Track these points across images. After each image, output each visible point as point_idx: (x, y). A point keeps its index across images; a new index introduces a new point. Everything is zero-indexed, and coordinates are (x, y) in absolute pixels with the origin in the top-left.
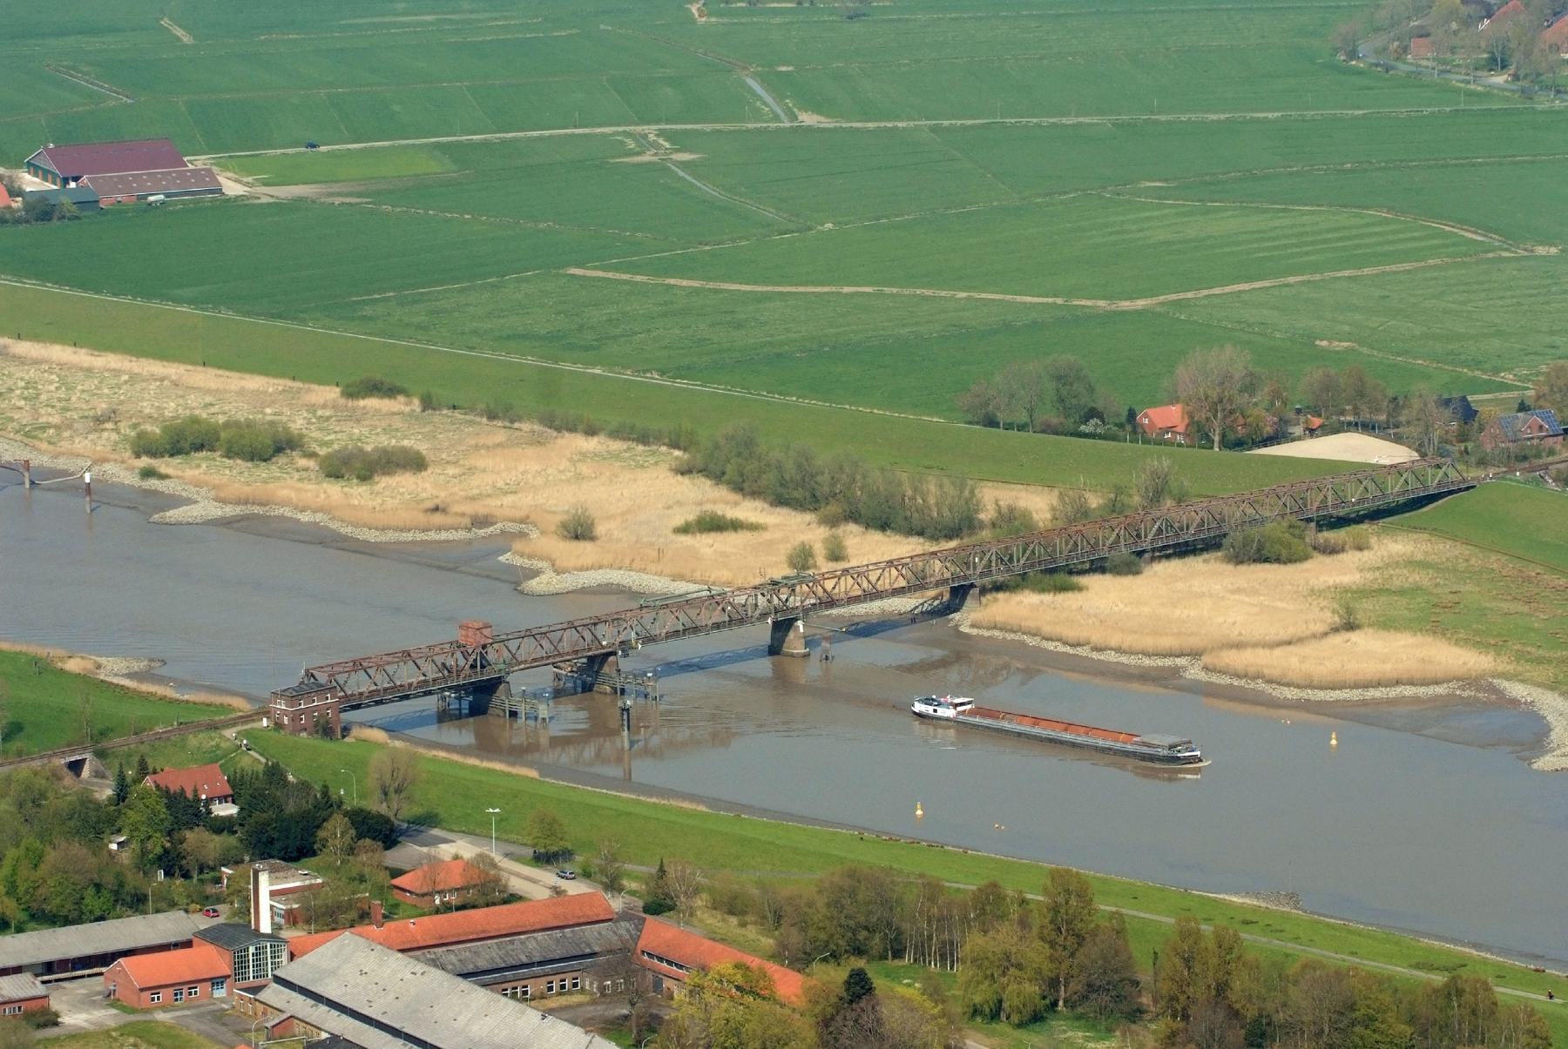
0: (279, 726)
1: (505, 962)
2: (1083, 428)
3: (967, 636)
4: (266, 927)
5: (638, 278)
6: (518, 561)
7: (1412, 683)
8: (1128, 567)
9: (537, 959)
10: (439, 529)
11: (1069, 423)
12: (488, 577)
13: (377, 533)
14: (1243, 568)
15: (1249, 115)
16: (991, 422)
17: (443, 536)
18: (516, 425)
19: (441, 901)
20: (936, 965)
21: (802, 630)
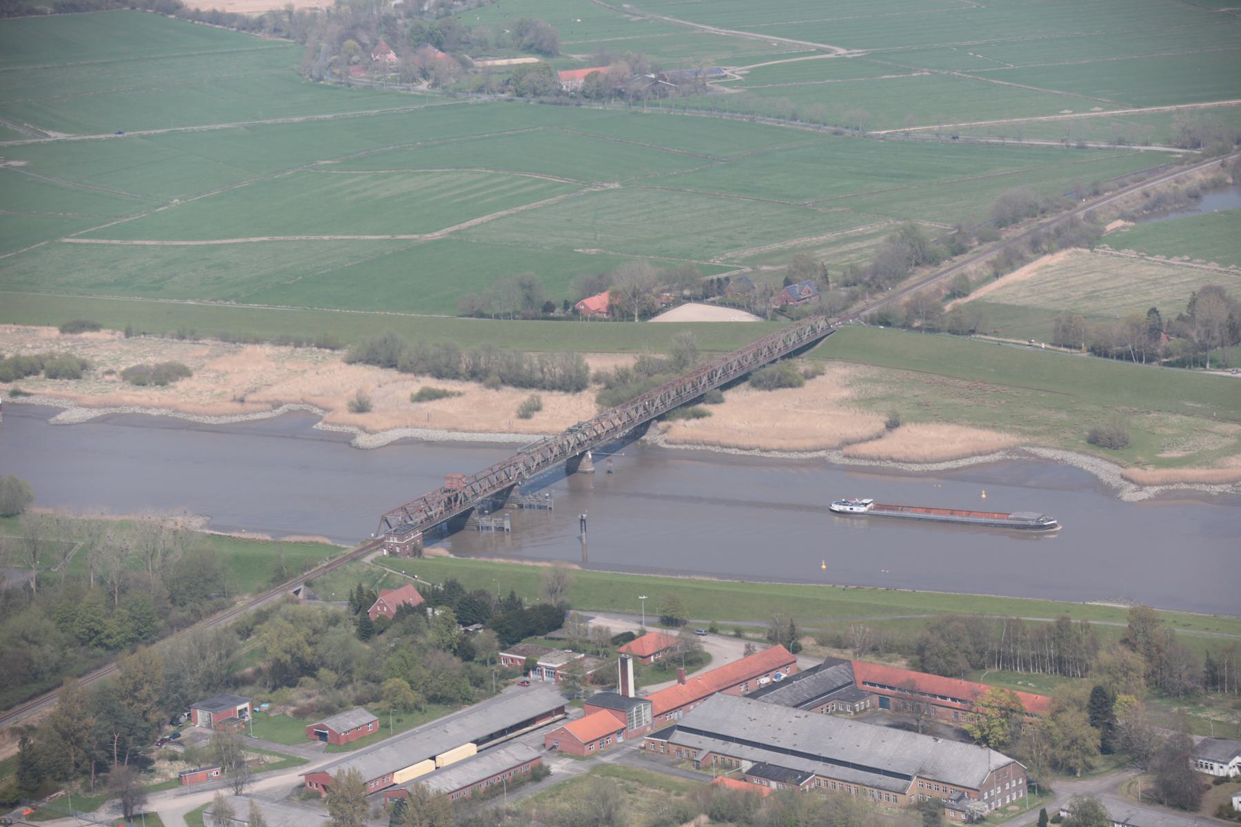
0: (392, 553)
1: (799, 699)
2: (552, 314)
3: (664, 449)
4: (632, 694)
5: (114, 242)
6: (329, 428)
7: (980, 454)
8: (718, 401)
9: (814, 695)
10: (254, 412)
12: (322, 440)
13: (217, 418)
14: (774, 392)
15: (316, 117)
16: (482, 315)
17: (258, 416)
18: (201, 342)
19: (654, 659)
20: (1021, 669)
21: (590, 456)
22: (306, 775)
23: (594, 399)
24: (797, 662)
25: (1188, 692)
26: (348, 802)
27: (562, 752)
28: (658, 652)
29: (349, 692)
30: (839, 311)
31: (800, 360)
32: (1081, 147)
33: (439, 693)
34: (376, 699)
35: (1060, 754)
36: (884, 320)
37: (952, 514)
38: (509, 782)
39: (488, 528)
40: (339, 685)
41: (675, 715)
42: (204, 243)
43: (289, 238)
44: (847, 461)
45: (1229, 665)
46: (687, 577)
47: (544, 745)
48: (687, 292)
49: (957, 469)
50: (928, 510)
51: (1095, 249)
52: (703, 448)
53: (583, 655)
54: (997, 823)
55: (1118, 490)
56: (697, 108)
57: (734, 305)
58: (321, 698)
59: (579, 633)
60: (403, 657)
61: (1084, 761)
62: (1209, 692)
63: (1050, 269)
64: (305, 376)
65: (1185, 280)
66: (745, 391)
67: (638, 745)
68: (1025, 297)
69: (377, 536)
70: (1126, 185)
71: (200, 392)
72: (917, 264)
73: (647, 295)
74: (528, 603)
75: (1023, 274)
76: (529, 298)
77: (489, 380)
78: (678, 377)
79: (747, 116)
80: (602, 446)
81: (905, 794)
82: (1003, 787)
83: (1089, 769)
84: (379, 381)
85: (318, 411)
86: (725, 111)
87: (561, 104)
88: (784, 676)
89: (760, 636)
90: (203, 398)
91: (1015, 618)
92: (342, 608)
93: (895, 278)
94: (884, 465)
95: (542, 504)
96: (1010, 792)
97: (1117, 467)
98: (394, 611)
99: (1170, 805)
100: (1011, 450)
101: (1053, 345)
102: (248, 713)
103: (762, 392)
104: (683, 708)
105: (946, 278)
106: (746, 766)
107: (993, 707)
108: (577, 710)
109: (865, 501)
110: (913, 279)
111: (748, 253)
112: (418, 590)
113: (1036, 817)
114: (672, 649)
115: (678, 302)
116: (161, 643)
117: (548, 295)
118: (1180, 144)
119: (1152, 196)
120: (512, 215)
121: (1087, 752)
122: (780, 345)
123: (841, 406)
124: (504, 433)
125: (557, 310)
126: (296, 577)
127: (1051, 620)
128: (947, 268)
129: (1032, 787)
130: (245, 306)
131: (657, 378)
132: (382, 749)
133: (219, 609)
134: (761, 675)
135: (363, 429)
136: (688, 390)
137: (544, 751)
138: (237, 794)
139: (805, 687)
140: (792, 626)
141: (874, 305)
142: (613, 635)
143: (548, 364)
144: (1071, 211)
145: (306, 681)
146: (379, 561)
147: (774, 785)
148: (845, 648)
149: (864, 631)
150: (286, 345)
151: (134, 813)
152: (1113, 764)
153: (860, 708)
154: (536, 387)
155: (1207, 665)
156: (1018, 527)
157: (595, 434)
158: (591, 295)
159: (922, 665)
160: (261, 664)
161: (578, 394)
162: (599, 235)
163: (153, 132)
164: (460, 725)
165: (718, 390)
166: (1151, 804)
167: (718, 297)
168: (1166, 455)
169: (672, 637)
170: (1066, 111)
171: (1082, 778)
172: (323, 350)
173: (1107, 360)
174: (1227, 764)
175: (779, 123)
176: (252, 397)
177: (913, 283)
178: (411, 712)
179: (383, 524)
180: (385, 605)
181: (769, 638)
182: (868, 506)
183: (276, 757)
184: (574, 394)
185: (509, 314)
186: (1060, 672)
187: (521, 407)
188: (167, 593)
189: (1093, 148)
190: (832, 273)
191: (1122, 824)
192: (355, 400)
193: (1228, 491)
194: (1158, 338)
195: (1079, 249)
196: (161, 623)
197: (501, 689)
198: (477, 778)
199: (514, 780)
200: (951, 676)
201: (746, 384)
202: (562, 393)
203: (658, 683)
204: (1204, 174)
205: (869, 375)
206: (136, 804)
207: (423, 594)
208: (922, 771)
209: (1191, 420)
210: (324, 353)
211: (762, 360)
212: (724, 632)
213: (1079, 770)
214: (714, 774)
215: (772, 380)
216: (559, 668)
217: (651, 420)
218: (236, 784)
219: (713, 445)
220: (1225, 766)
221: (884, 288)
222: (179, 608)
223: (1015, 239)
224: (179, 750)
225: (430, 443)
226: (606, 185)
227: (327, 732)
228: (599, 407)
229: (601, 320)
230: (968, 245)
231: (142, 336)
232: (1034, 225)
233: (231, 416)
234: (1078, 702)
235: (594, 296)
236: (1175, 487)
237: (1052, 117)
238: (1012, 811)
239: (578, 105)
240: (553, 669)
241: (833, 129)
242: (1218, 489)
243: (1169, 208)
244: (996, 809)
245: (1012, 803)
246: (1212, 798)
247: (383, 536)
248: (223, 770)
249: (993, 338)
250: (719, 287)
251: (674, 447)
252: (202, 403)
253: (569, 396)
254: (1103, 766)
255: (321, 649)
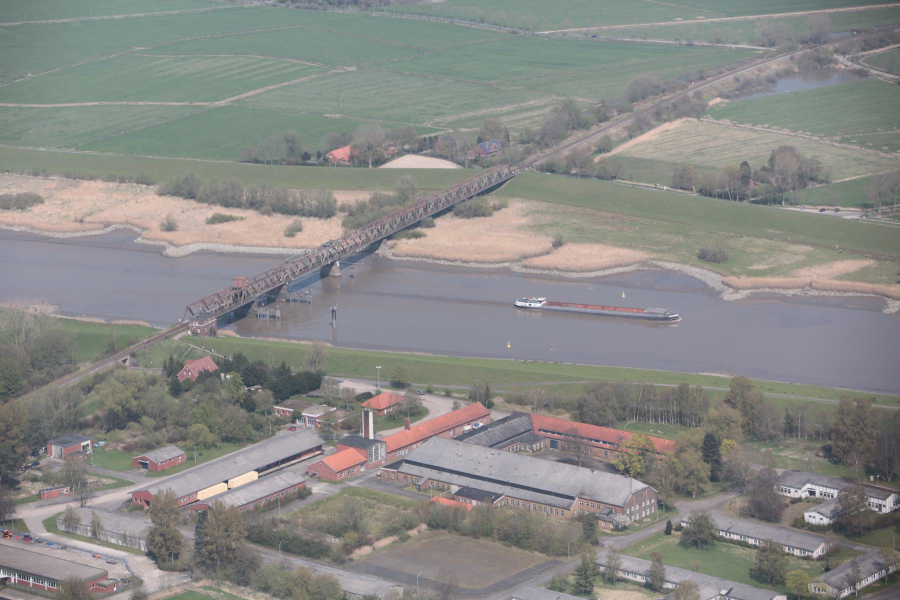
0: (194, 333)
1: (493, 441)
2: (308, 161)
4: (371, 437)
6: (146, 242)
7: (621, 266)
8: (431, 225)
9: (503, 439)
10: (91, 230)
11: (301, 162)
12: (141, 251)
14: (471, 219)
16: (257, 162)
17: (93, 233)
18: (50, 178)
20: (652, 421)
21: (338, 265)
22: (134, 493)
23: (340, 223)
24: (491, 415)
25: (771, 438)
26: (165, 513)
27: (320, 478)
28: (390, 407)
29: (163, 434)
30: (518, 162)
31: (490, 197)
32: (690, 45)
33: (230, 435)
34: (184, 439)
35: (681, 482)
36: (550, 168)
37: (603, 309)
38: (282, 499)
39: (264, 316)
40: (156, 429)
41: (402, 453)
42: (51, 106)
43: (114, 103)
44: (524, 270)
45: (802, 419)
46: (410, 353)
47: (307, 473)
48: (406, 147)
49: (604, 276)
50: (586, 306)
51: (701, 119)
52: (420, 259)
53: (335, 408)
54: (636, 531)
55: (720, 293)
56: (412, 14)
57: (440, 156)
58: (144, 438)
59: (332, 393)
60: (204, 408)
61: (698, 487)
62: (787, 437)
63: (669, 133)
64: (128, 204)
65: (766, 142)
66: (450, 219)
67: (376, 473)
68: (651, 153)
69: (183, 321)
70: (723, 73)
71: (51, 215)
72: (574, 128)
73: (378, 148)
74: (295, 370)
75: (649, 136)
76: (292, 150)
77: (263, 209)
78: (400, 208)
79: (448, 19)
80: (346, 257)
81: (569, 510)
82: (640, 505)
83: (701, 493)
84: (182, 208)
85: (138, 229)
86: (432, 16)
87: (312, 9)
88: (481, 424)
89: (463, 396)
90: (53, 219)
91: (648, 384)
92: (158, 372)
93: (558, 138)
94: (551, 273)
95: (303, 299)
96: (645, 509)
97: (719, 276)
98: (196, 375)
99: (759, 518)
100: (643, 263)
101: (672, 187)
102: (90, 448)
103: (463, 220)
104: (408, 447)
105: (594, 138)
106: (455, 489)
107: (633, 448)
108: (331, 448)
109: (540, 299)
110: (571, 139)
111: (450, 119)
112: (214, 360)
113: (664, 526)
114: (399, 404)
115: (400, 154)
116: (25, 397)
117: (305, 148)
118: (760, 43)
119: (741, 80)
120: (278, 89)
121: (701, 480)
122: (476, 185)
123: (520, 230)
124: (275, 247)
125: (312, 159)
126: (124, 350)
127: (674, 386)
128: (596, 131)
129: (661, 505)
130: (82, 152)
131: (387, 208)
132: (188, 475)
133: (67, 373)
134: (465, 424)
135: (171, 243)
136: (409, 217)
137: (307, 477)
138: (82, 506)
139: (497, 432)
140: (487, 389)
141: (542, 157)
142: (357, 394)
143: (307, 198)
144: (683, 91)
145: (132, 425)
146: (185, 339)
147: (474, 502)
148: (525, 405)
149: (540, 393)
150: (113, 181)
151: (6, 519)
152: (719, 489)
153: (536, 447)
154: (298, 214)
155: (786, 419)
156: (650, 319)
157: (342, 249)
158: (336, 148)
159: (581, 418)
160: (100, 413)
161: (329, 219)
162: (342, 104)
163: (11, 24)
164: (246, 458)
165: (431, 218)
166: (745, 518)
167: (429, 151)
168: (755, 267)
169: (400, 396)
170: (679, 19)
171: (697, 499)
172: (142, 185)
173: (711, 198)
174: (800, 489)
175: (471, 25)
176: (88, 219)
177: (572, 142)
178: (209, 448)
179: (187, 313)
180: (191, 371)
181: (470, 397)
182: (542, 303)
183: (110, 480)
184: (325, 220)
185: (277, 161)
186: (680, 423)
187: (287, 228)
188: (29, 361)
189: (698, 45)
190: (512, 134)
191: (726, 531)
192: (165, 222)
193: (799, 293)
194: (747, 183)
195: (690, 119)
196: (24, 382)
197: (275, 432)
198: (258, 496)
199: (285, 498)
200: (602, 425)
201: (451, 213)
202: (317, 219)
203: (390, 429)
204: (778, 65)
205: (540, 208)
206: (7, 513)
207: (218, 363)
208: (582, 493)
209: (772, 242)
210: (142, 187)
211: (462, 197)
212: (437, 393)
213: (695, 493)
214: (431, 495)
215: (470, 212)
216: (318, 418)
217: (382, 239)
218: (82, 499)
219: (427, 257)
220: (799, 491)
221: (550, 145)
222: (38, 371)
223: (644, 111)
224: (39, 474)
225: (221, 254)
226: (346, 68)
227: (148, 462)
228: (344, 229)
229: (344, 166)
230: (610, 115)
231: (7, 173)
232: (658, 100)
233: (73, 232)
234: (695, 445)
235: (339, 148)
236: (761, 290)
237: (668, 23)
238: (647, 522)
239: (324, 10)
240: (313, 418)
241: (510, 29)
242: (791, 292)
243: (753, 89)
244: (635, 521)
245: (646, 516)
246: (790, 513)
247: (188, 321)
248: (71, 489)
249: (629, 182)
250: (430, 143)
251: (399, 258)
252: (52, 222)
253: (322, 221)
254: (712, 490)
255: (143, 402)
